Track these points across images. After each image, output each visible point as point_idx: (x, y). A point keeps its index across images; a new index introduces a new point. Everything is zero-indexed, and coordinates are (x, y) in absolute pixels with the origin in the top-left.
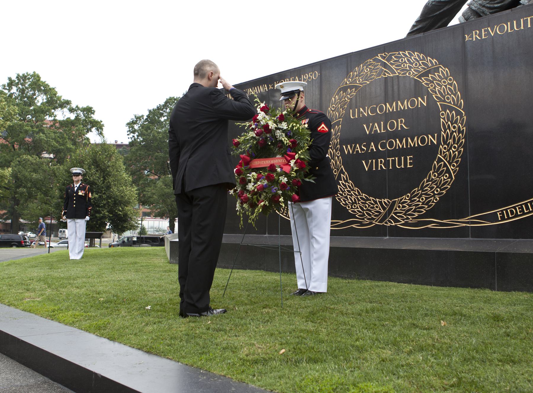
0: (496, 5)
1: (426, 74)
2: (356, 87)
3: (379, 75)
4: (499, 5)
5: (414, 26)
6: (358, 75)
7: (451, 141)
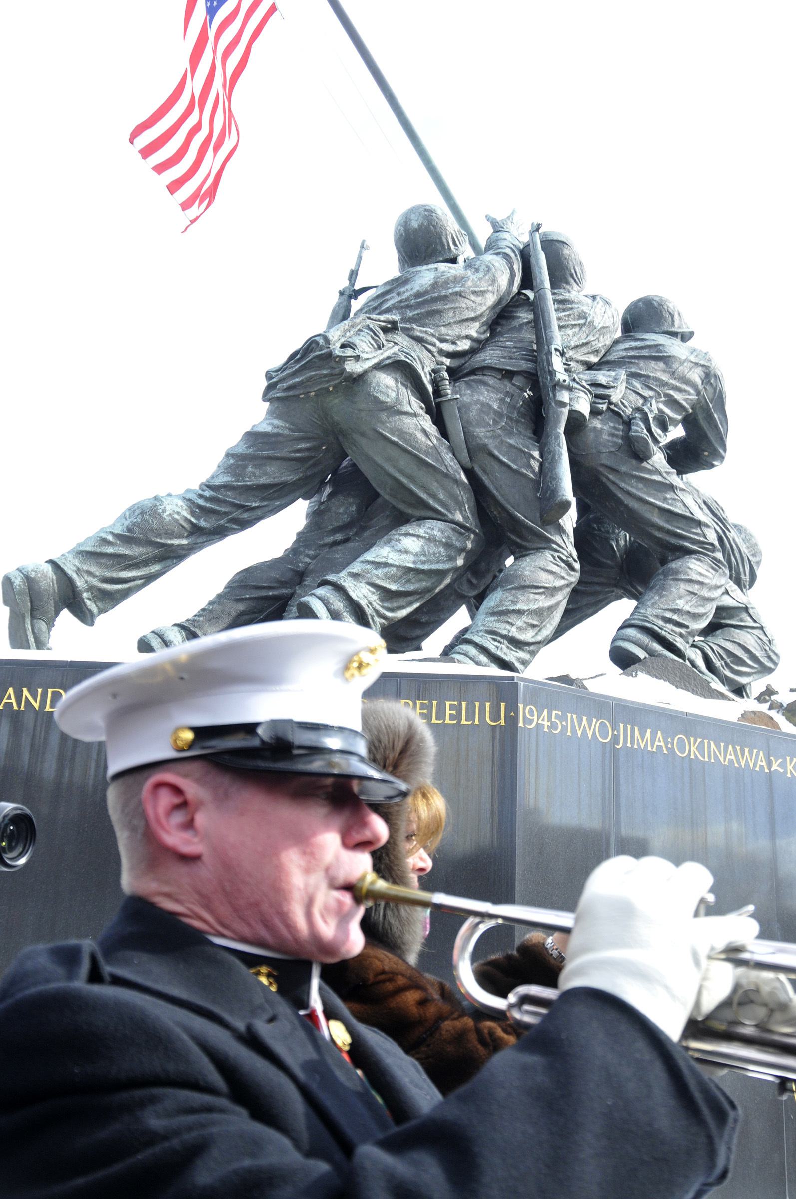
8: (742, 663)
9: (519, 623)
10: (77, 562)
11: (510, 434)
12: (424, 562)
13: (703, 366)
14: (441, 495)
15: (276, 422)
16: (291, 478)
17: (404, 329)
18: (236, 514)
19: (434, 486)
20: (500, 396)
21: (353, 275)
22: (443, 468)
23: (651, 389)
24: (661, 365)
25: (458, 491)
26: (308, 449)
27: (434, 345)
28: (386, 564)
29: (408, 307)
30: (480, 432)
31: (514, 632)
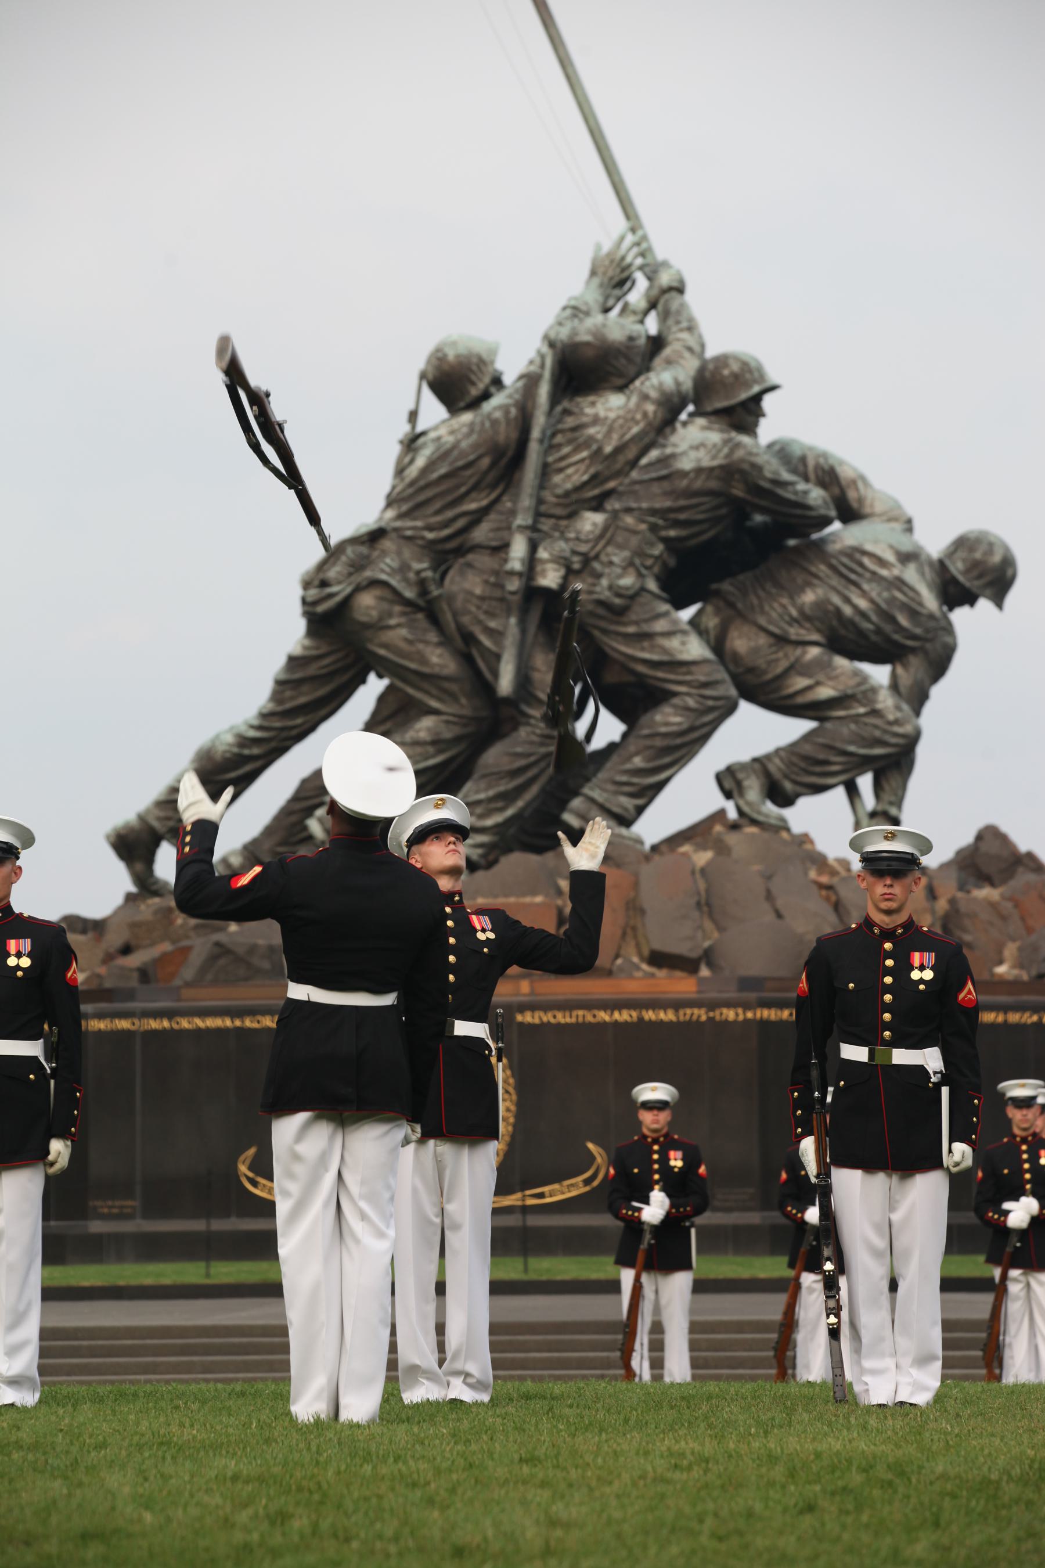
8: (827, 763)
11: (491, 614)
16: (322, 692)
17: (396, 530)
18: (284, 734)
19: (426, 685)
20: (485, 577)
21: (413, 416)
23: (643, 521)
24: (666, 485)
25: (446, 685)
26: (335, 662)
27: (423, 538)
30: (465, 620)
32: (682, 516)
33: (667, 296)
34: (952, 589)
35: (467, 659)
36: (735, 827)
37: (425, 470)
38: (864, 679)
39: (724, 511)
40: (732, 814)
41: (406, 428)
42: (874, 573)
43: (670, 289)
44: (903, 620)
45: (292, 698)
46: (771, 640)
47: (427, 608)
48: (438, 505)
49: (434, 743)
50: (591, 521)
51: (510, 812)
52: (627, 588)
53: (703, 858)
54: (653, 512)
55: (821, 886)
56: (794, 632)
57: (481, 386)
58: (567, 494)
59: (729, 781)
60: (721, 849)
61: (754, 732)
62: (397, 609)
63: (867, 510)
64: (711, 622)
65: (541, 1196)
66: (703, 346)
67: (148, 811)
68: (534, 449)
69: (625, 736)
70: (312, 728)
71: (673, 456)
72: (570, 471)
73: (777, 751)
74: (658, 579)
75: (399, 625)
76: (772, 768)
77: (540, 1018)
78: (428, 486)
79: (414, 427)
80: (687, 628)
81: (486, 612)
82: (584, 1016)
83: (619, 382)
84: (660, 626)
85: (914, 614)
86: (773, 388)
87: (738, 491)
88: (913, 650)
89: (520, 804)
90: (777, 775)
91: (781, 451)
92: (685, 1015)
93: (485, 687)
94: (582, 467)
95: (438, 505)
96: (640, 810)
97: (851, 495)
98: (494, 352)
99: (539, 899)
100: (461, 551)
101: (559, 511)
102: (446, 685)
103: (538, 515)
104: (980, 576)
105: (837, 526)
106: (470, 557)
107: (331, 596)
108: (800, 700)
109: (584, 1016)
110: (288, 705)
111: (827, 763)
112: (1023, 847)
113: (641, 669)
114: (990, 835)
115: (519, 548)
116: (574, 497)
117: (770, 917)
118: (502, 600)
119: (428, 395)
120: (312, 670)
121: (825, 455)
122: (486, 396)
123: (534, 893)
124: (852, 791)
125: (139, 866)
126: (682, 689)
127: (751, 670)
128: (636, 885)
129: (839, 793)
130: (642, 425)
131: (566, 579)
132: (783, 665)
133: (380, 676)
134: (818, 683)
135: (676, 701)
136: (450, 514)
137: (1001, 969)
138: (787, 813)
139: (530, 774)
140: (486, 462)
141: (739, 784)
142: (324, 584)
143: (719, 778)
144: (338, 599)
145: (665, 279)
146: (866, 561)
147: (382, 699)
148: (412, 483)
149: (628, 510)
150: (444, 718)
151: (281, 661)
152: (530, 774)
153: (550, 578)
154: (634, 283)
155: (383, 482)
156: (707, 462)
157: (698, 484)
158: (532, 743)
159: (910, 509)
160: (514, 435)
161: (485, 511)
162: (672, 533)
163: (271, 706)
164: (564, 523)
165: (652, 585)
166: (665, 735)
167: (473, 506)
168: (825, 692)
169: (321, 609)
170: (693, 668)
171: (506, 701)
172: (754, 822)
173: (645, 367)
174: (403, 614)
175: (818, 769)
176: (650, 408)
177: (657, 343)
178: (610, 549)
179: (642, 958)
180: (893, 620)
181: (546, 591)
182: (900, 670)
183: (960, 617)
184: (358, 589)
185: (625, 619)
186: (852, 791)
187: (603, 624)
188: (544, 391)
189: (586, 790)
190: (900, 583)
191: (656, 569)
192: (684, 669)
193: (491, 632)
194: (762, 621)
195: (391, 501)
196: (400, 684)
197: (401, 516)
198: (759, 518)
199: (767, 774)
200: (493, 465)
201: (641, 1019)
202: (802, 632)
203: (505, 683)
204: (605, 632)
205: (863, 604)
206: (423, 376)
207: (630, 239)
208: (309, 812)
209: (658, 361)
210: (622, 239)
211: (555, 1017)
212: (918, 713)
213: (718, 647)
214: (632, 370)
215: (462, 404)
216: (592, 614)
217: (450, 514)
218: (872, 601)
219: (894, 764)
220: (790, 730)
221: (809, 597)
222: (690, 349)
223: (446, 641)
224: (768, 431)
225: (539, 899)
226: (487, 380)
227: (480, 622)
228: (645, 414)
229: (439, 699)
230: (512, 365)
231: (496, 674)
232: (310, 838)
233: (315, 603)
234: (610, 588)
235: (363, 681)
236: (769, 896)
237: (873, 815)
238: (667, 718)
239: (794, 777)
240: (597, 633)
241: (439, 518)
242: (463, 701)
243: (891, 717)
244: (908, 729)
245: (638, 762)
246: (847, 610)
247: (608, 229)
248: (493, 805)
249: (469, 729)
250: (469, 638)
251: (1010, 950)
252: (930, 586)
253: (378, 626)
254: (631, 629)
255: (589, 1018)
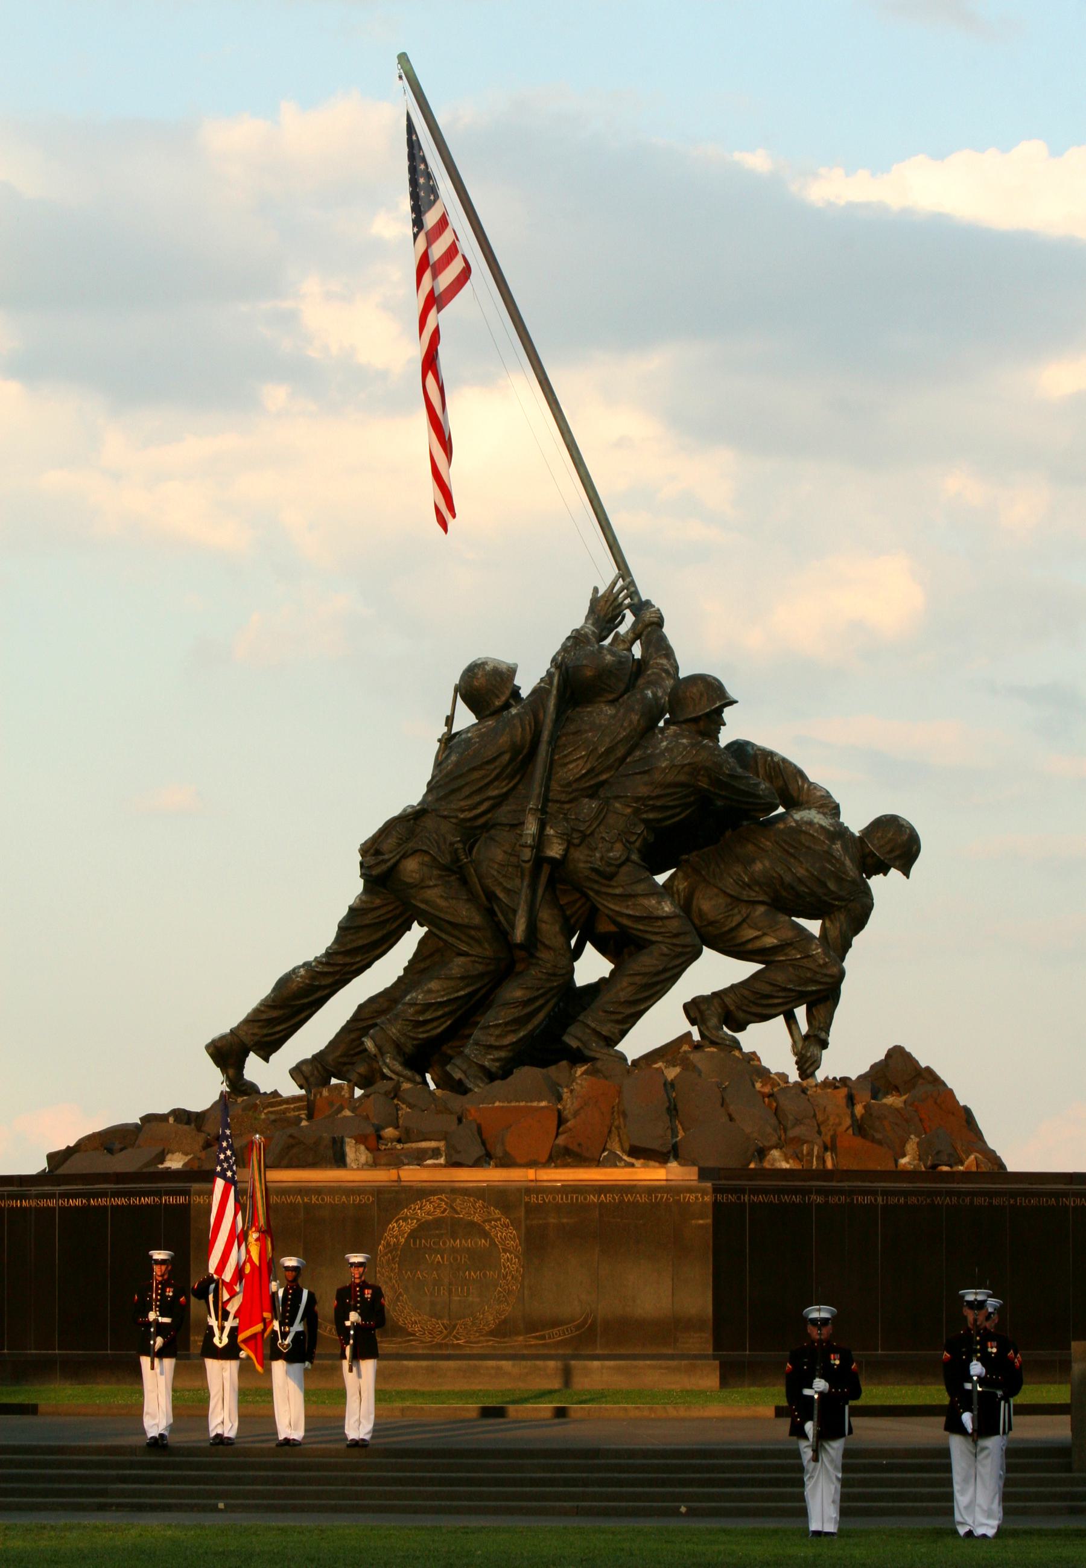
0: (421, 1036)
1: (489, 1221)
2: (418, 1220)
3: (443, 1212)
4: (425, 1036)
5: (257, 1011)
6: (420, 1209)
7: (509, 1278)
9: (497, 1032)
10: (245, 1028)
12: (443, 996)
13: (689, 764)
14: (464, 938)
15: (364, 898)
17: (433, 810)
18: (347, 969)
19: (456, 933)
21: (449, 721)
22: (459, 921)
24: (646, 778)
25: (473, 933)
27: (456, 817)
28: (416, 1004)
29: (440, 786)
30: (489, 882)
31: (492, 1041)
32: (659, 803)
33: (651, 627)
34: (869, 861)
35: (491, 913)
36: (697, 1047)
37: (457, 764)
38: (802, 930)
39: (692, 799)
40: (696, 1037)
41: (445, 729)
42: (808, 848)
43: (652, 624)
44: (832, 886)
45: (353, 941)
46: (729, 900)
47: (456, 871)
48: (467, 791)
49: (462, 978)
50: (590, 806)
51: (522, 1034)
52: (616, 859)
53: (672, 1073)
54: (637, 799)
55: (764, 1095)
56: (745, 895)
57: (503, 698)
58: (569, 784)
59: (694, 1010)
60: (686, 1065)
61: (714, 972)
62: (436, 872)
63: (804, 798)
64: (682, 885)
65: (543, 1337)
66: (677, 668)
67: (239, 1026)
68: (543, 748)
69: (612, 973)
70: (369, 965)
71: (651, 756)
72: (571, 766)
73: (733, 987)
74: (640, 851)
75: (435, 886)
76: (727, 1000)
77: (543, 1200)
78: (461, 776)
79: (450, 729)
80: (662, 890)
81: (504, 876)
82: (577, 1198)
83: (611, 697)
84: (640, 888)
85: (840, 880)
86: (732, 703)
87: (704, 784)
88: (839, 908)
89: (530, 1027)
90: (732, 1008)
91: (739, 748)
92: (656, 1197)
93: (502, 934)
94: (581, 762)
95: (467, 791)
96: (623, 1033)
97: (792, 788)
98: (512, 671)
99: (543, 1104)
100: (486, 827)
101: (563, 797)
102: (473, 933)
103: (546, 800)
104: (891, 851)
105: (781, 810)
106: (493, 832)
107: (385, 861)
108: (750, 946)
109: (577, 1198)
110: (349, 947)
111: (772, 997)
112: (923, 1065)
113: (626, 922)
114: (898, 1056)
115: (531, 827)
116: (575, 786)
117: (725, 1119)
118: (517, 866)
119: (460, 704)
120: (368, 920)
121: (771, 754)
122: (507, 706)
123: (540, 1100)
124: (791, 1020)
125: (231, 1072)
126: (659, 938)
127: (711, 923)
128: (620, 1093)
129: (781, 1018)
130: (628, 730)
131: (567, 850)
132: (737, 919)
133: (421, 925)
134: (765, 934)
135: (654, 947)
136: (477, 798)
137: (904, 1161)
138: (739, 1036)
139: (537, 1004)
140: (506, 757)
141: (701, 1012)
142: (378, 853)
143: (687, 1008)
144: (389, 864)
145: (648, 616)
146: (803, 838)
147: (422, 942)
148: (447, 775)
149: (617, 797)
150: (473, 959)
151: (344, 911)
152: (537, 1004)
153: (555, 851)
154: (624, 617)
155: (424, 772)
156: (678, 761)
157: (670, 778)
158: (540, 979)
159: (837, 797)
160: (528, 738)
161: (505, 796)
162: (651, 816)
163: (336, 947)
164: (567, 806)
165: (635, 857)
166: (644, 974)
167: (496, 792)
168: (770, 941)
169: (374, 873)
170: (666, 922)
171: (520, 946)
172: (713, 1043)
173: (631, 686)
174: (440, 877)
175: (765, 1002)
176: (635, 718)
177: (640, 666)
178: (602, 828)
179: (623, 1151)
180: (825, 885)
181: (552, 860)
182: (828, 924)
183: (876, 883)
184: (404, 856)
185: (613, 883)
186: (791, 1020)
187: (596, 887)
188: (552, 703)
189: (581, 1018)
190: (829, 855)
191: (638, 844)
192: (660, 923)
193: (508, 891)
194: (720, 885)
195: (431, 787)
196: (435, 930)
197: (438, 800)
198: (719, 803)
199: (725, 1006)
200: (511, 760)
201: (621, 1201)
202: (754, 894)
203: (519, 933)
204: (597, 892)
205: (801, 872)
206: (457, 689)
207: (620, 583)
208: (365, 1031)
209: (641, 682)
210: (614, 583)
211: (554, 1198)
212: (843, 959)
213: (686, 907)
214: (622, 687)
215: (488, 713)
216: (588, 878)
217: (477, 798)
218: (807, 870)
219: (824, 996)
220: (742, 970)
221: (758, 866)
222: (667, 671)
223: (472, 898)
224: (725, 738)
225: (543, 1104)
226: (508, 693)
227: (500, 884)
228: (631, 722)
229: (469, 944)
230: (526, 683)
231: (513, 926)
232: (365, 1050)
233: (369, 867)
234: (602, 859)
235: (409, 929)
236: (723, 1103)
237: (807, 1037)
238: (647, 962)
239: (745, 1008)
240: (591, 893)
241: (469, 802)
242: (486, 946)
243: (821, 962)
244: (834, 970)
245: (623, 996)
246: (788, 879)
247: (605, 575)
248: (509, 1028)
249: (491, 967)
250: (491, 896)
251: (911, 1147)
252: (851, 860)
253: (420, 886)
254: (618, 891)
255: (581, 1199)
